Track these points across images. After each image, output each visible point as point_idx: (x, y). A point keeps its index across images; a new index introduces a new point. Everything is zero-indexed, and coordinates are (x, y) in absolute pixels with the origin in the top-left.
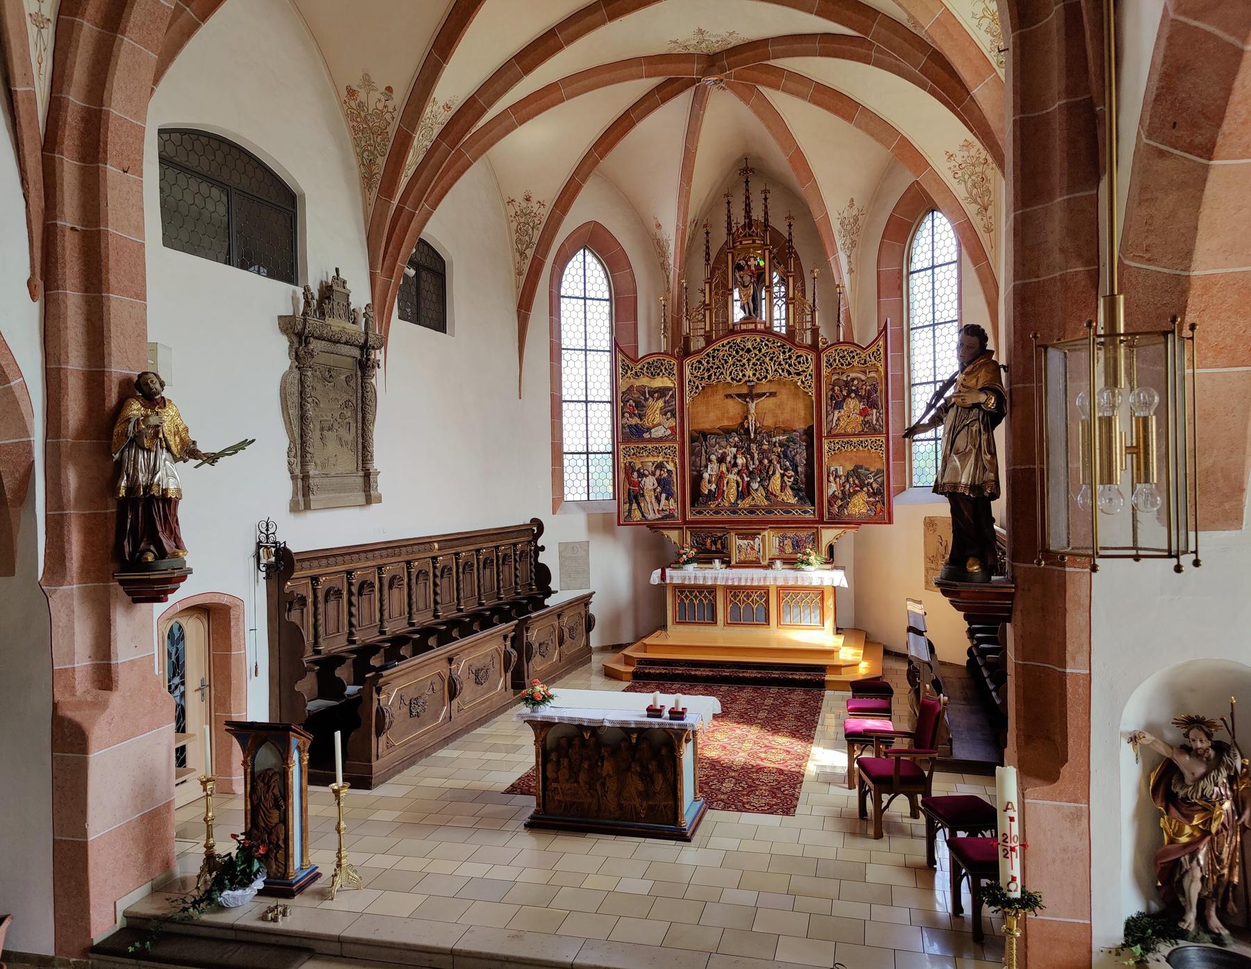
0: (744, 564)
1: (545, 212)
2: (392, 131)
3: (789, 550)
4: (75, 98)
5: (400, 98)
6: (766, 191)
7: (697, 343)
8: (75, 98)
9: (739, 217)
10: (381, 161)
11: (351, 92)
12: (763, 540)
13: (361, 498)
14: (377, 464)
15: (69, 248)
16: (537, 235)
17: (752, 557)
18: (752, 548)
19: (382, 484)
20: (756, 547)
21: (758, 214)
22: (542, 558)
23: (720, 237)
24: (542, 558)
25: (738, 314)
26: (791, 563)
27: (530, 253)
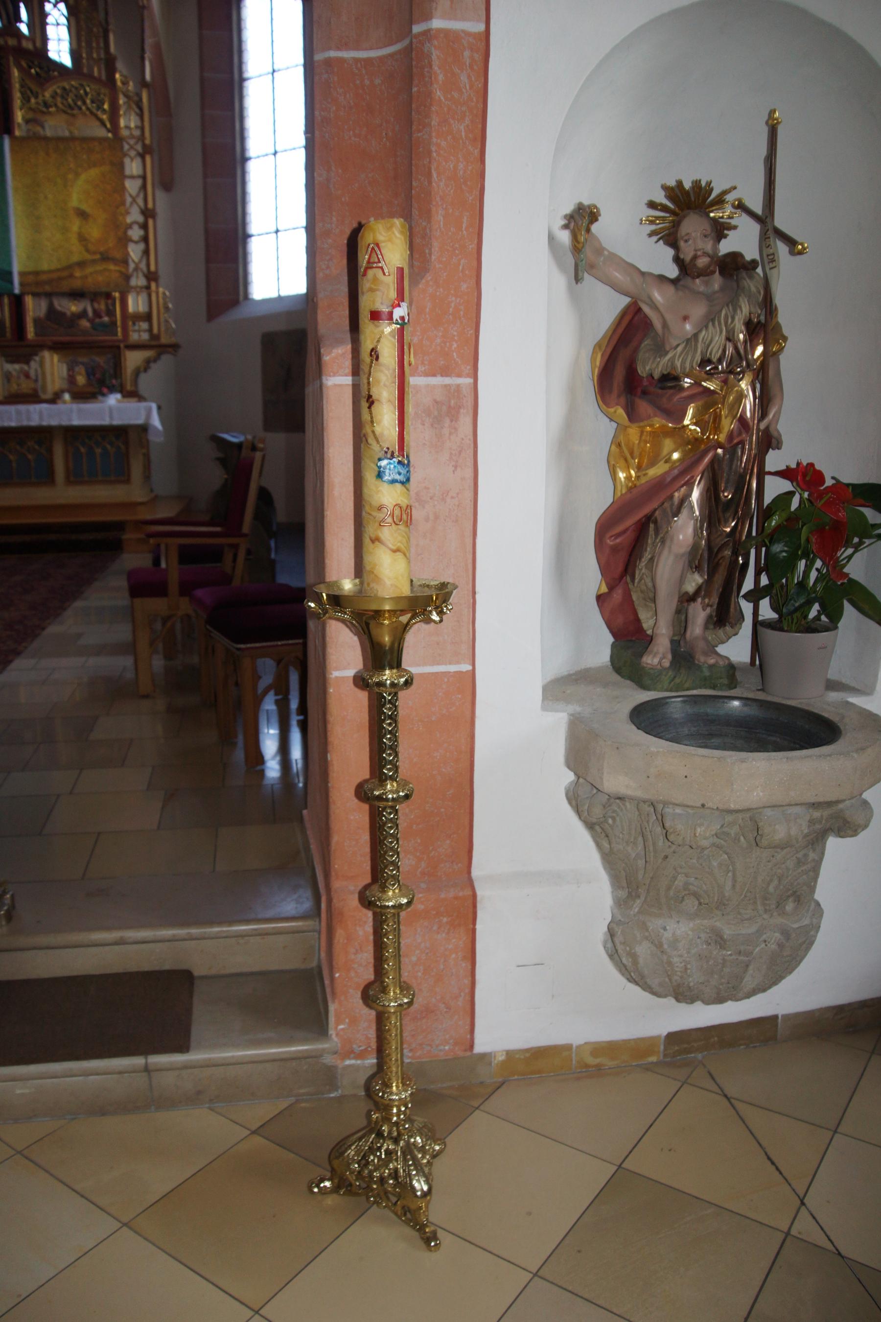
3: (81, 380)
12: (42, 364)
17: (26, 386)
18: (27, 376)
20: (32, 374)
26: (80, 396)
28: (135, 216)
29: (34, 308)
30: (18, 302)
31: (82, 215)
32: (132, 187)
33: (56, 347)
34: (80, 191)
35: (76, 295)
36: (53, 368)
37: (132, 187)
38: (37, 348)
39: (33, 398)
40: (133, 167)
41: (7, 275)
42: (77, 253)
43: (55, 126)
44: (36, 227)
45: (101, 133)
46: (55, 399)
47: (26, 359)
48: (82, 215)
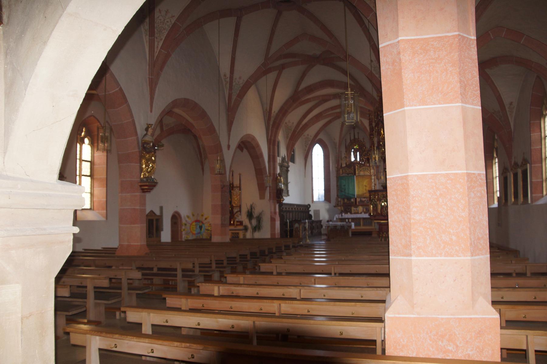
0: (355, 213)
1: (312, 138)
2: (293, 129)
4: (273, 138)
5: (295, 124)
6: (358, 133)
7: (343, 166)
8: (273, 138)
9: (352, 138)
10: (290, 134)
11: (286, 123)
13: (286, 195)
14: (289, 189)
15: (271, 157)
16: (309, 142)
19: (290, 193)
21: (356, 137)
22: (310, 213)
23: (348, 141)
24: (310, 213)
25: (353, 159)
27: (308, 146)
28: (373, 185)
29: (358, 200)
30: (356, 199)
31: (366, 186)
32: (373, 181)
33: (361, 205)
34: (365, 182)
35: (364, 198)
36: (360, 209)
37: (373, 181)
38: (359, 206)
39: (358, 213)
40: (373, 177)
41: (354, 195)
42: (365, 191)
43: (362, 173)
44: (359, 188)
45: (369, 174)
46: (361, 213)
47: (356, 207)
48: (366, 186)
